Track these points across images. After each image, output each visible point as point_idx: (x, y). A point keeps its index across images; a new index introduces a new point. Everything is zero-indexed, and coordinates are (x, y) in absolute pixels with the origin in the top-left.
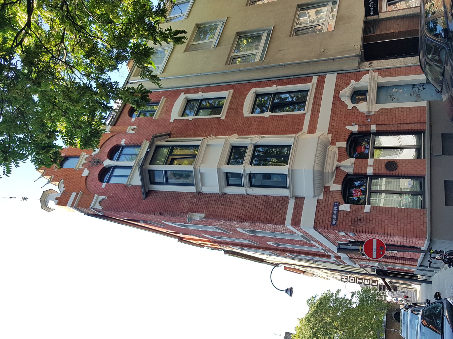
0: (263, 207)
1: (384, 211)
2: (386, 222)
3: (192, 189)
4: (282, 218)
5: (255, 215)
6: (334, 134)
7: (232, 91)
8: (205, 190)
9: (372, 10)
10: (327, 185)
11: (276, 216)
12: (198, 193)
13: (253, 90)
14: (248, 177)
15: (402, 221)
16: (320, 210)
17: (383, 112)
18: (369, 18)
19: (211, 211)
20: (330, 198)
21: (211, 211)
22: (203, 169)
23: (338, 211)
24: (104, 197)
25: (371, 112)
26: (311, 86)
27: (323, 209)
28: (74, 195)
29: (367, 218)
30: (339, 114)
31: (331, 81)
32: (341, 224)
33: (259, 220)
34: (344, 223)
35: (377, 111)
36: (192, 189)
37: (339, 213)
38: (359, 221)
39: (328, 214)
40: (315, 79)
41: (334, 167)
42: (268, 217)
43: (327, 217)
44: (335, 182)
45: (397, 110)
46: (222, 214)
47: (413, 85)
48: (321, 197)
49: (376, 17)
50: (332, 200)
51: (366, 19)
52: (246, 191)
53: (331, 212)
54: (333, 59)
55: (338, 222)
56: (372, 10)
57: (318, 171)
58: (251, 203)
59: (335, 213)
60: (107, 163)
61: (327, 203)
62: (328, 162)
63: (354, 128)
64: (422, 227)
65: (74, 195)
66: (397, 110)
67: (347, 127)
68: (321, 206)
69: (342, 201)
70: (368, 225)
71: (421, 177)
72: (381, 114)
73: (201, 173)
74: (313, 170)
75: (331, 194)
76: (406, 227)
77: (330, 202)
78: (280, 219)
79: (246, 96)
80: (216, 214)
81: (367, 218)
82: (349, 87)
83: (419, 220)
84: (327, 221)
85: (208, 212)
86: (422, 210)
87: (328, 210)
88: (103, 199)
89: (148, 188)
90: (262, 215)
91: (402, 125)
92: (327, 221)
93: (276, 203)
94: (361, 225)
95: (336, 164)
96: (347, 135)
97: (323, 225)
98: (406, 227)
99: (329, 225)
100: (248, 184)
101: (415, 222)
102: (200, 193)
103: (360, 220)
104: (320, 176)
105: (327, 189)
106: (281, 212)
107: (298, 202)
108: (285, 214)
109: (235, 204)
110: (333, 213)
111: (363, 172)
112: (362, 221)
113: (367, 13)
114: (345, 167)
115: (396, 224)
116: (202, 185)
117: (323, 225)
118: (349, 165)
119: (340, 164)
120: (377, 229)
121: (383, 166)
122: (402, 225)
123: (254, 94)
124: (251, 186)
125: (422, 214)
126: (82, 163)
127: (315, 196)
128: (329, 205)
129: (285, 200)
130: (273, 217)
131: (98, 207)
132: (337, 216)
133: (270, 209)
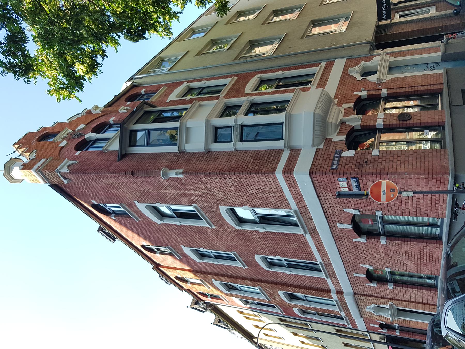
0: (252, 160)
1: (396, 153)
2: (399, 162)
3: (174, 149)
4: (273, 167)
5: (241, 167)
6: (340, 99)
7: (236, 78)
8: (189, 148)
9: (384, 13)
10: (329, 137)
11: (266, 165)
12: (180, 153)
13: (258, 76)
14: (239, 130)
15: (419, 160)
16: (319, 157)
17: (394, 80)
18: (382, 23)
19: (191, 166)
20: (331, 147)
21: (191, 166)
22: (190, 123)
23: (340, 156)
25: (382, 80)
26: (318, 70)
27: (322, 156)
28: (43, 160)
29: (375, 161)
30: (347, 85)
32: (343, 168)
33: (245, 171)
34: (347, 166)
35: (389, 80)
36: (174, 149)
37: (342, 159)
38: (365, 164)
39: (328, 160)
40: (323, 64)
41: (339, 121)
42: (257, 168)
43: (327, 163)
44: (339, 134)
45: (410, 78)
46: (203, 169)
47: (427, 64)
48: (321, 147)
49: (388, 22)
50: (334, 148)
51: (379, 23)
52: (235, 145)
53: (332, 158)
54: (344, 47)
55: (340, 166)
56: (384, 13)
57: (320, 115)
58: (239, 157)
59: (337, 159)
60: (90, 135)
61: (327, 151)
62: (332, 114)
63: (363, 93)
64: (443, 164)
65: (43, 160)
66: (410, 78)
67: (354, 93)
68: (320, 154)
69: (346, 148)
70: (376, 166)
71: (439, 126)
72: (393, 81)
73: (187, 128)
74: (314, 113)
75: (333, 144)
76: (423, 165)
77: (331, 150)
78: (270, 169)
80: (196, 168)
81: (375, 161)
82: (359, 66)
83: (439, 158)
84: (326, 166)
85: (188, 167)
86: (443, 150)
87: (329, 156)
89: (126, 151)
90: (249, 166)
91: (416, 88)
92: (326, 166)
93: (267, 155)
94: (368, 167)
95: (341, 117)
96: (355, 99)
97: (321, 170)
98: (423, 165)
99: (328, 171)
100: (238, 138)
101: (435, 160)
102: (182, 152)
103: (366, 162)
104: (321, 123)
105: (328, 141)
106: (272, 162)
107: (293, 153)
108: (277, 163)
109: (220, 159)
110: (334, 159)
111: (371, 124)
112: (369, 163)
113: (380, 18)
114: (349, 120)
115: (410, 164)
116: (187, 142)
117: (321, 170)
118: (356, 121)
119: (346, 118)
120: (386, 169)
121: (395, 118)
122: (418, 164)
123: (259, 79)
124: (242, 141)
125: (442, 152)
126: (63, 137)
127: (313, 145)
128: (330, 153)
129: (279, 152)
130: (263, 167)
131: (65, 170)
132: (339, 160)
133: (259, 161)
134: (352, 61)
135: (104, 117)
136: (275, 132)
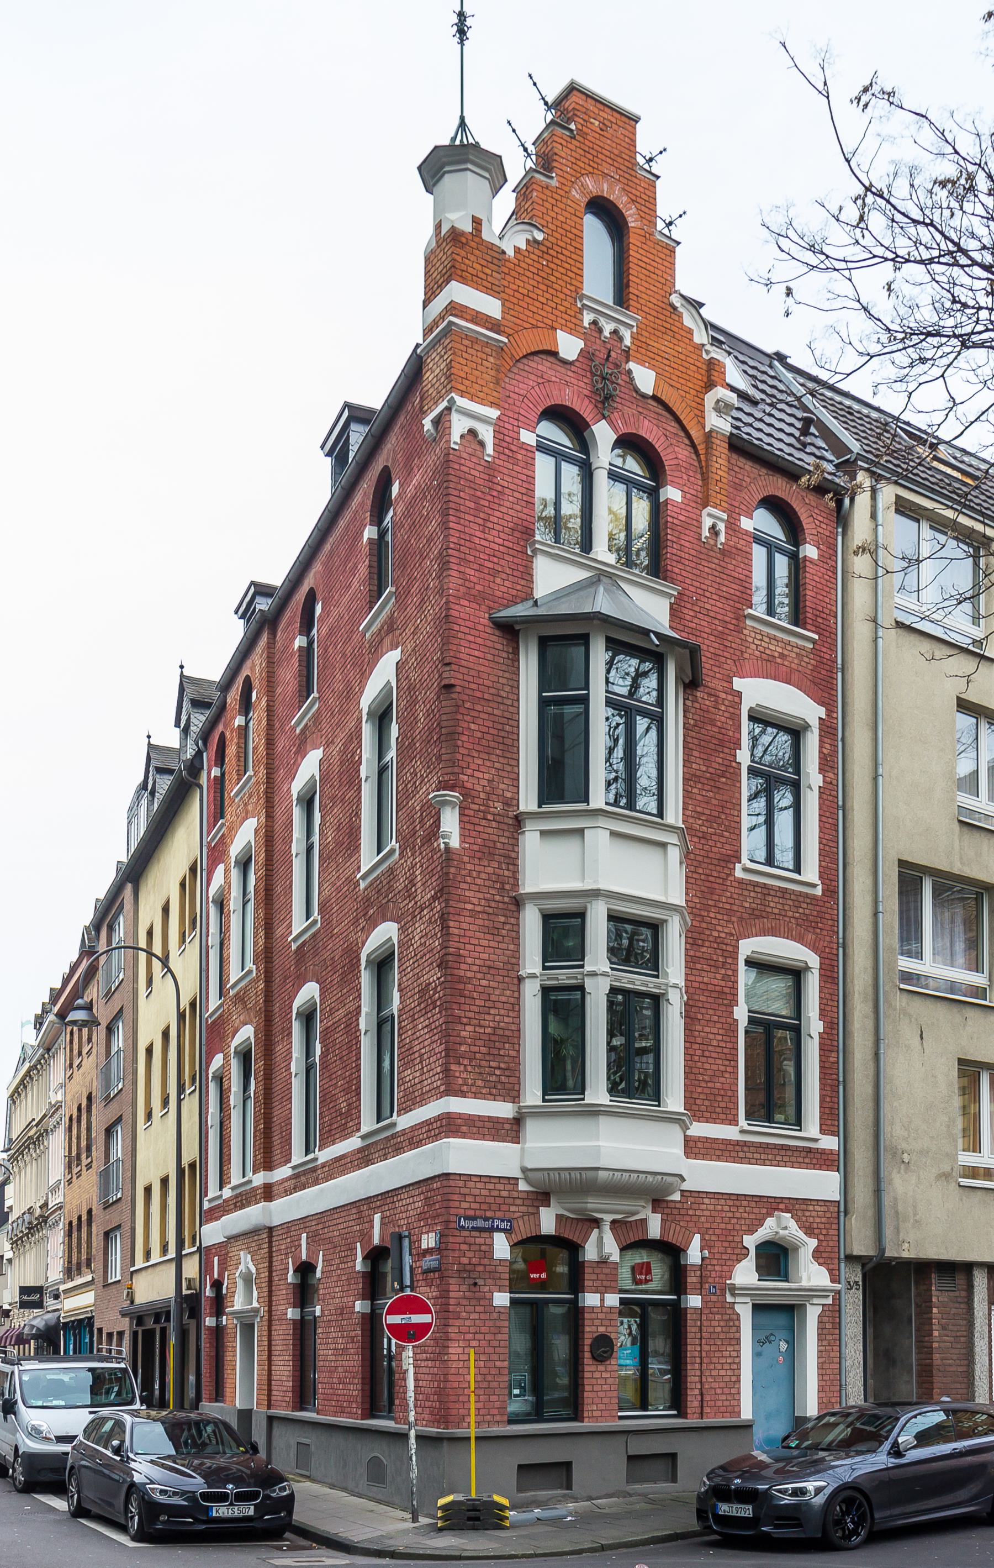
0: (488, 1030)
4: (465, 1088)
8: (531, 841)
11: (469, 1068)
13: (813, 960)
16: (491, 1186)
19: (469, 867)
20: (521, 1209)
21: (469, 867)
23: (492, 1230)
24: (490, 450)
27: (495, 1193)
29: (479, 1299)
30: (730, 1215)
31: (823, 1185)
32: (460, 1240)
34: (464, 1247)
36: (528, 800)
38: (472, 1281)
39: (484, 1207)
40: (830, 1143)
42: (463, 1048)
44: (559, 1218)
46: (461, 905)
52: (533, 976)
53: (489, 1214)
55: (467, 1233)
58: (497, 992)
59: (487, 1224)
61: (511, 1201)
63: (694, 1254)
66: (734, 1354)
68: (501, 1187)
69: (516, 1238)
70: (464, 1302)
72: (726, 1317)
73: (581, 832)
74: (598, 1169)
75: (531, 1210)
77: (513, 1208)
79: (800, 939)
81: (479, 1299)
82: (801, 1234)
84: (465, 1205)
85: (466, 859)
87: (494, 1207)
88: (482, 444)
90: (468, 1028)
92: (465, 1205)
93: (502, 1065)
102: (519, 821)
103: (475, 1284)
106: (480, 1083)
107: (507, 1126)
109: (493, 944)
110: (486, 1219)
116: (543, 833)
119: (607, 1228)
121: (602, 1329)
124: (546, 990)
127: (524, 1170)
128: (504, 1207)
129: (512, 1092)
132: (480, 1230)
133: (484, 1050)
134: (825, 1220)
135: (684, 453)
136: (563, 1074)
